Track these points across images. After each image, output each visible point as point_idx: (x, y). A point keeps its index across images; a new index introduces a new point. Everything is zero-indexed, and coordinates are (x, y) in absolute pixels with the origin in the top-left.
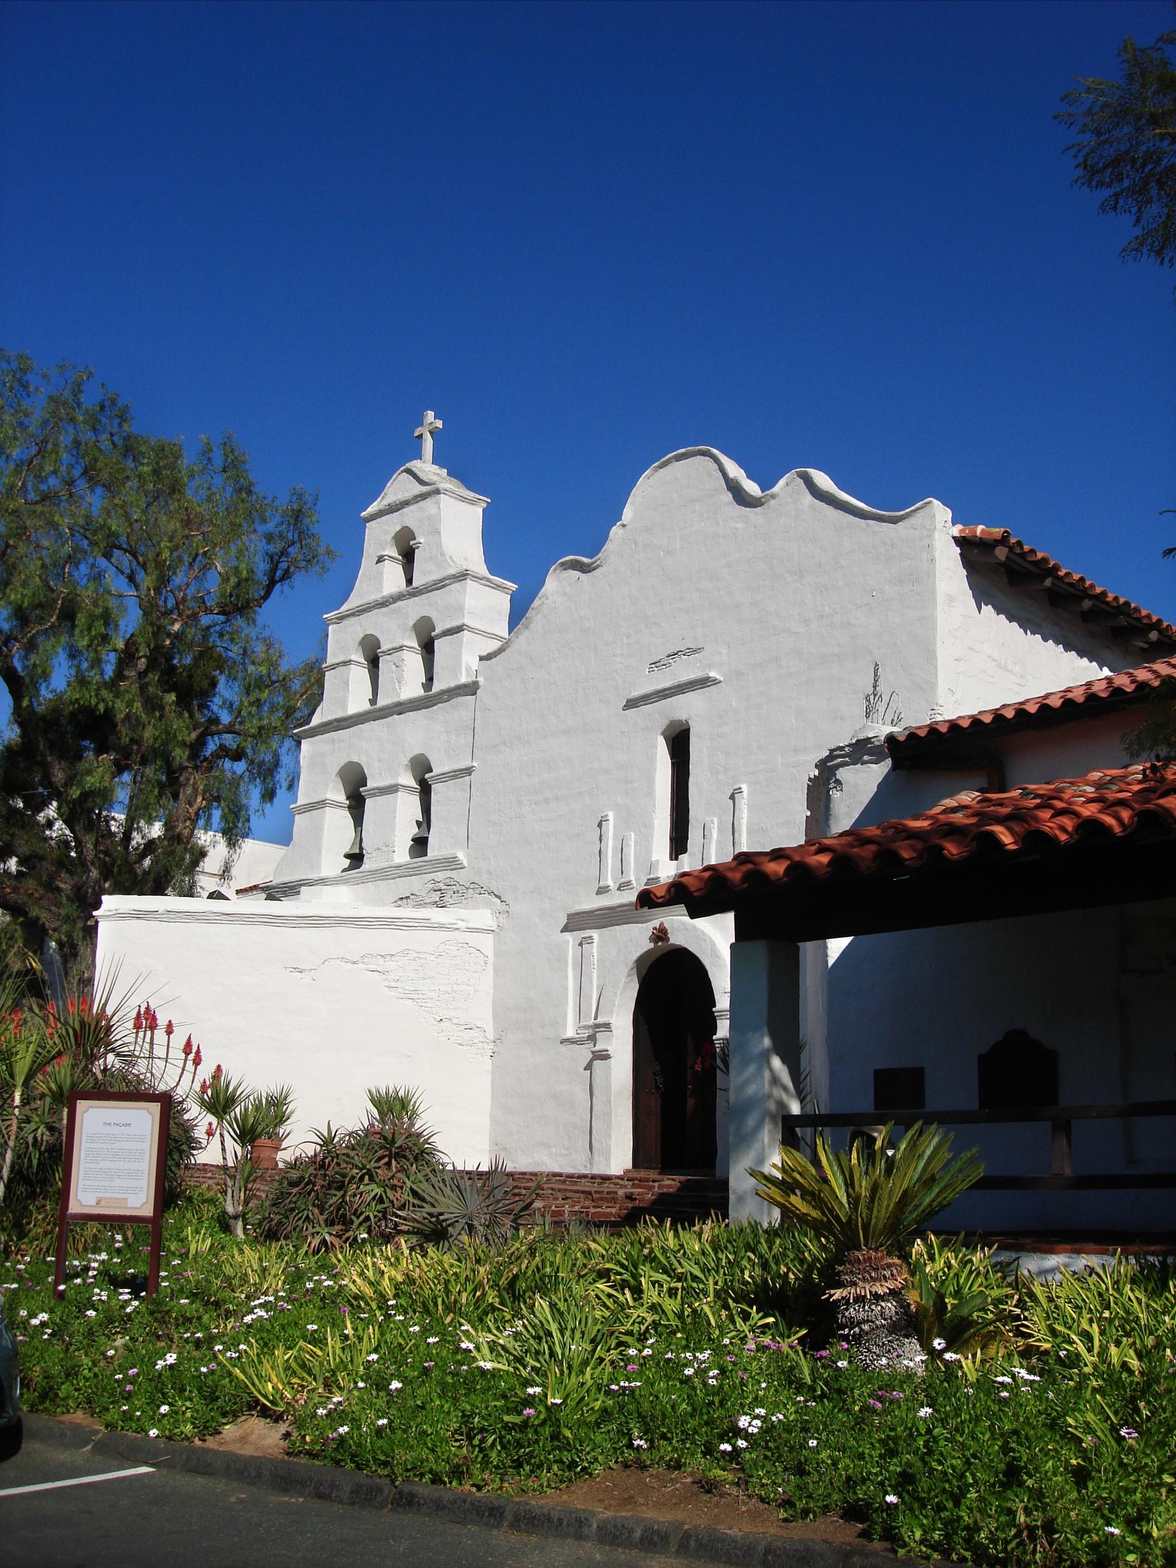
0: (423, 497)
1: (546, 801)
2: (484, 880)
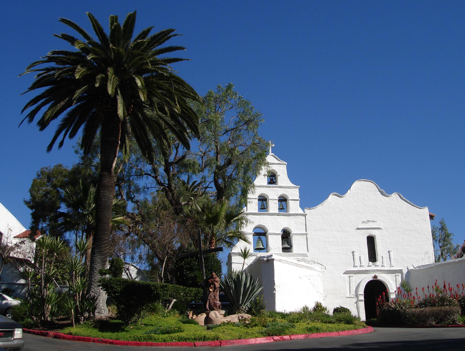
0: (280, 164)
1: (334, 245)
2: (316, 260)
